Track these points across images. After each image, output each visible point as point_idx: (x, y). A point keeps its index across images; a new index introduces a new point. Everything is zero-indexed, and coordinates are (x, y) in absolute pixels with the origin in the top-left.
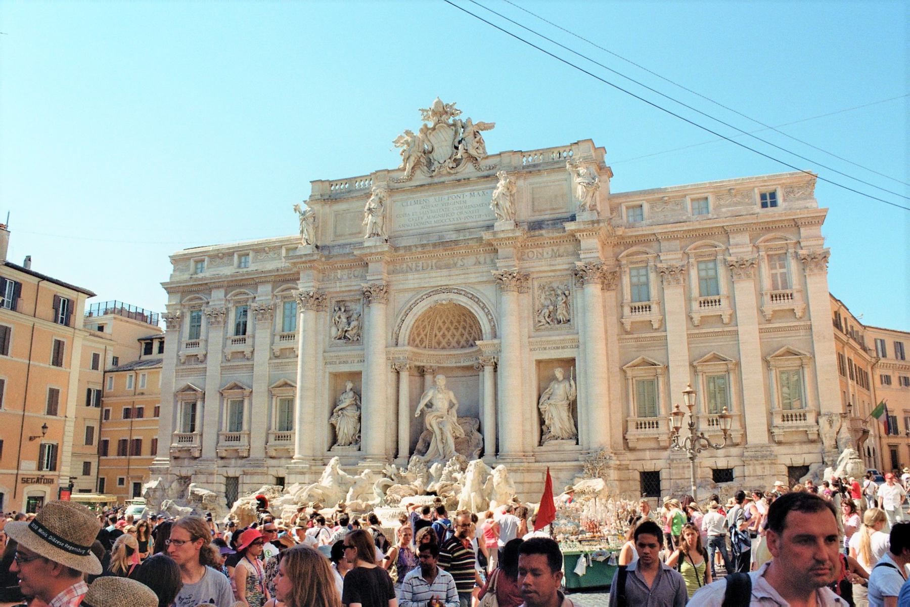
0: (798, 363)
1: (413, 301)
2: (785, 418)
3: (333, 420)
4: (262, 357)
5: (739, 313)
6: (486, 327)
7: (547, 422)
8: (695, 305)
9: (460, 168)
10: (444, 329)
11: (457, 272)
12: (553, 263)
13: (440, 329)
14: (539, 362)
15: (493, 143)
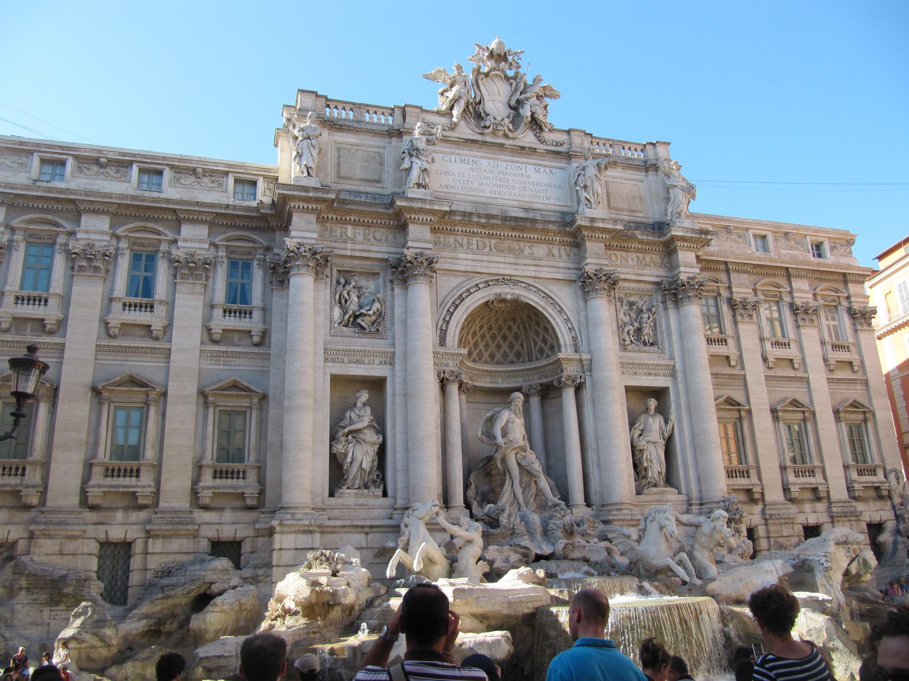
0: (861, 417)
1: (464, 289)
2: (860, 472)
3: (339, 448)
4: (187, 339)
5: (808, 360)
6: (564, 336)
7: (645, 464)
8: (768, 345)
9: (518, 134)
10: (478, 336)
11: (526, 261)
12: (641, 272)
13: (474, 334)
14: (629, 390)
15: (557, 116)
